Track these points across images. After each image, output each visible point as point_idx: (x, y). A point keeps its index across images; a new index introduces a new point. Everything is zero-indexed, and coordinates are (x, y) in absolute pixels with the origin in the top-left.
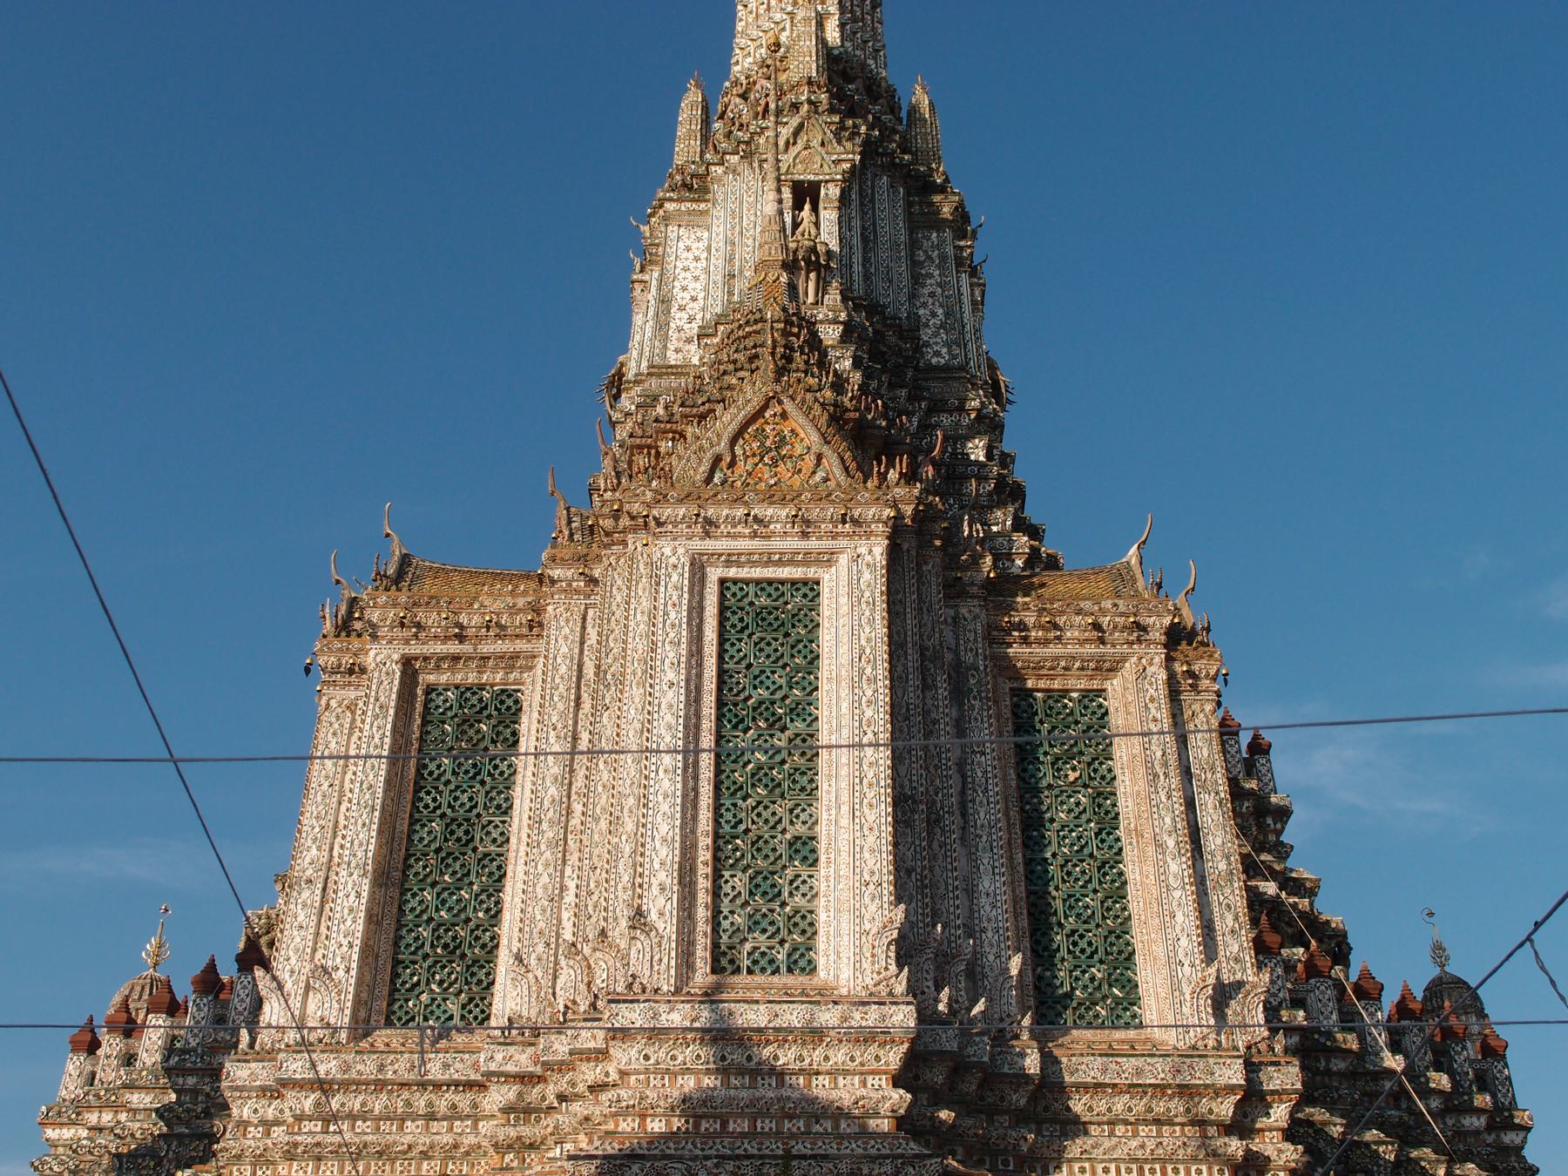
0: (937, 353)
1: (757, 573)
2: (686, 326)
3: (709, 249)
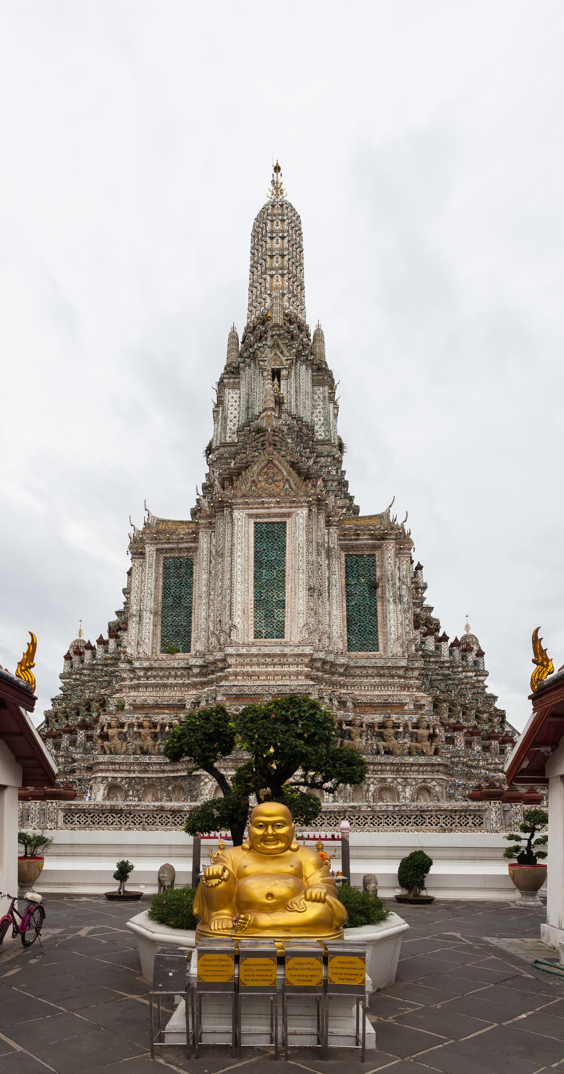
0: (321, 435)
1: (265, 520)
2: (233, 428)
3: (240, 397)
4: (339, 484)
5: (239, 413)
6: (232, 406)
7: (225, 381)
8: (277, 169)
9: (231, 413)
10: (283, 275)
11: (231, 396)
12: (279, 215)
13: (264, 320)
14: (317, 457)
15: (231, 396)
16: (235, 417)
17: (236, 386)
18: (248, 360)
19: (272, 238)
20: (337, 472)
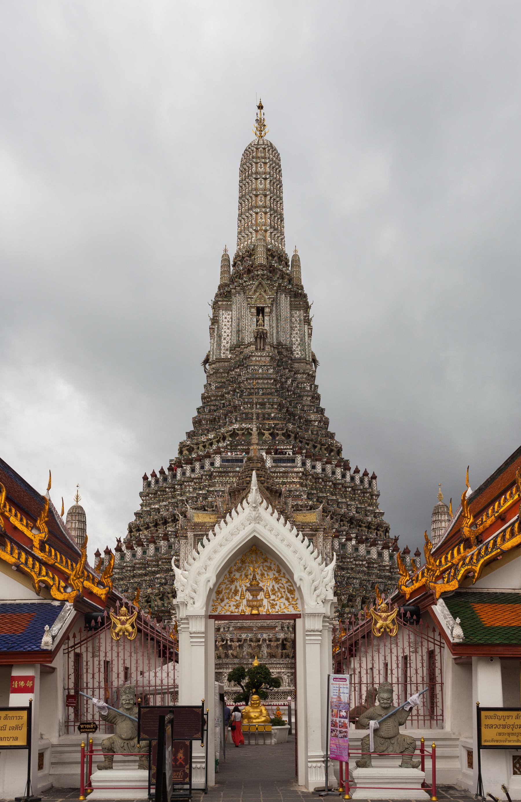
0: (298, 354)
3: (232, 318)
4: (313, 398)
5: (231, 332)
6: (225, 325)
7: (220, 303)
8: (260, 107)
9: (225, 332)
10: (266, 213)
11: (225, 317)
12: (263, 158)
13: (251, 253)
14: (295, 373)
15: (225, 317)
16: (228, 336)
17: (228, 308)
18: (238, 288)
19: (256, 179)
20: (311, 387)
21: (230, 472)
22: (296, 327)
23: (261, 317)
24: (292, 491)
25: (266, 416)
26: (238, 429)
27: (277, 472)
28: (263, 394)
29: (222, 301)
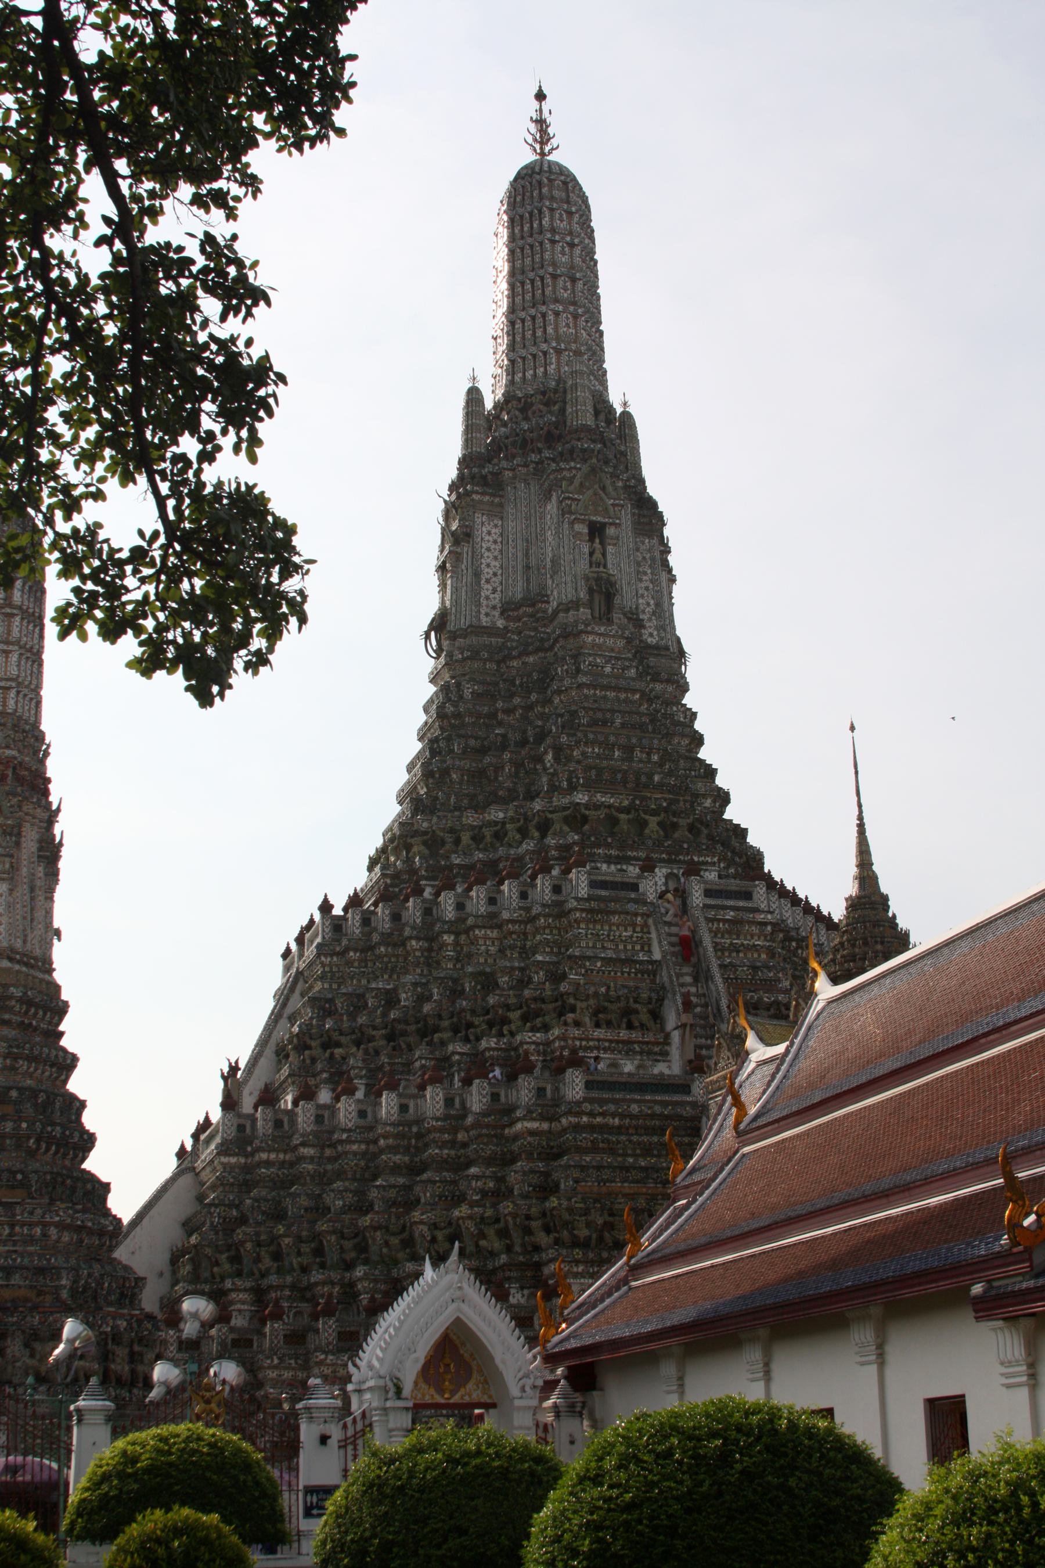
0: (651, 635)
6: (488, 549)
9: (488, 565)
11: (487, 531)
16: (495, 574)
17: (497, 511)
21: (614, 913)
22: (645, 573)
23: (597, 544)
24: (758, 968)
25: (643, 779)
26: (587, 806)
27: (719, 920)
28: (623, 725)
29: (482, 494)
